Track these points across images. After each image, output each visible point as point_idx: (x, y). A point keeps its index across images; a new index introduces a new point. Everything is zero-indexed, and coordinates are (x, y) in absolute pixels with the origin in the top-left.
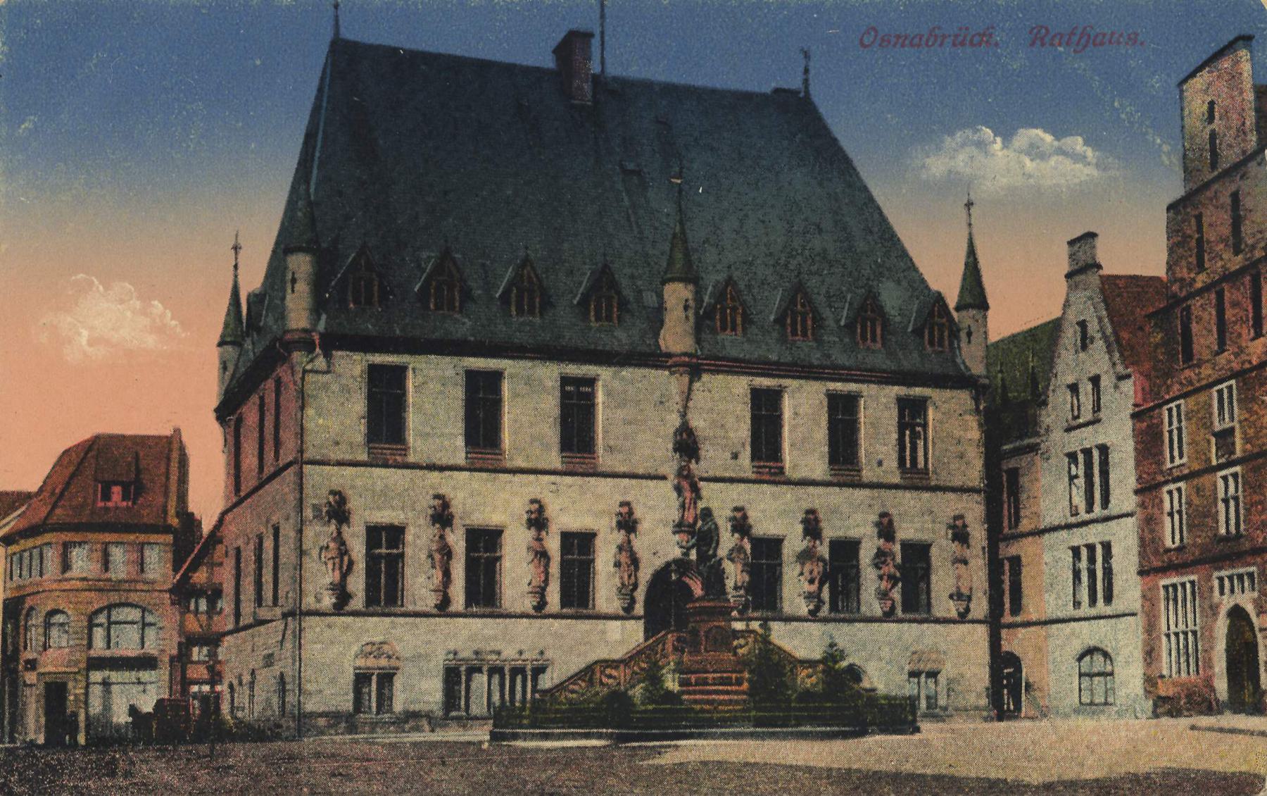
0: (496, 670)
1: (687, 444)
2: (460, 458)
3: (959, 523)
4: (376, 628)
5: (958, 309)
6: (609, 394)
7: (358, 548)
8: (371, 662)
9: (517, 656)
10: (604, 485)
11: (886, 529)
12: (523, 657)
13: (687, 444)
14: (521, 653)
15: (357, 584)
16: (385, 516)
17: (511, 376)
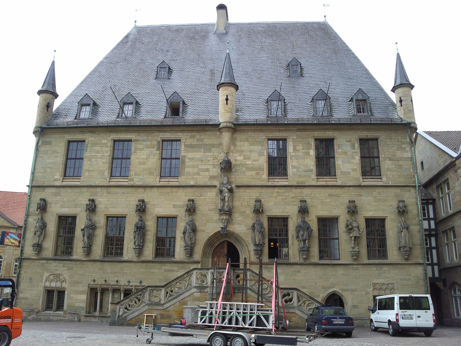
0: (115, 291)
1: (227, 167)
2: (104, 180)
3: (401, 205)
4: (58, 267)
5: (393, 90)
6: (185, 146)
7: (52, 227)
8: (53, 285)
9: (127, 284)
10: (181, 192)
11: (353, 210)
12: (131, 284)
13: (227, 167)
14: (129, 282)
15: (49, 245)
16: (66, 211)
17: (136, 140)
